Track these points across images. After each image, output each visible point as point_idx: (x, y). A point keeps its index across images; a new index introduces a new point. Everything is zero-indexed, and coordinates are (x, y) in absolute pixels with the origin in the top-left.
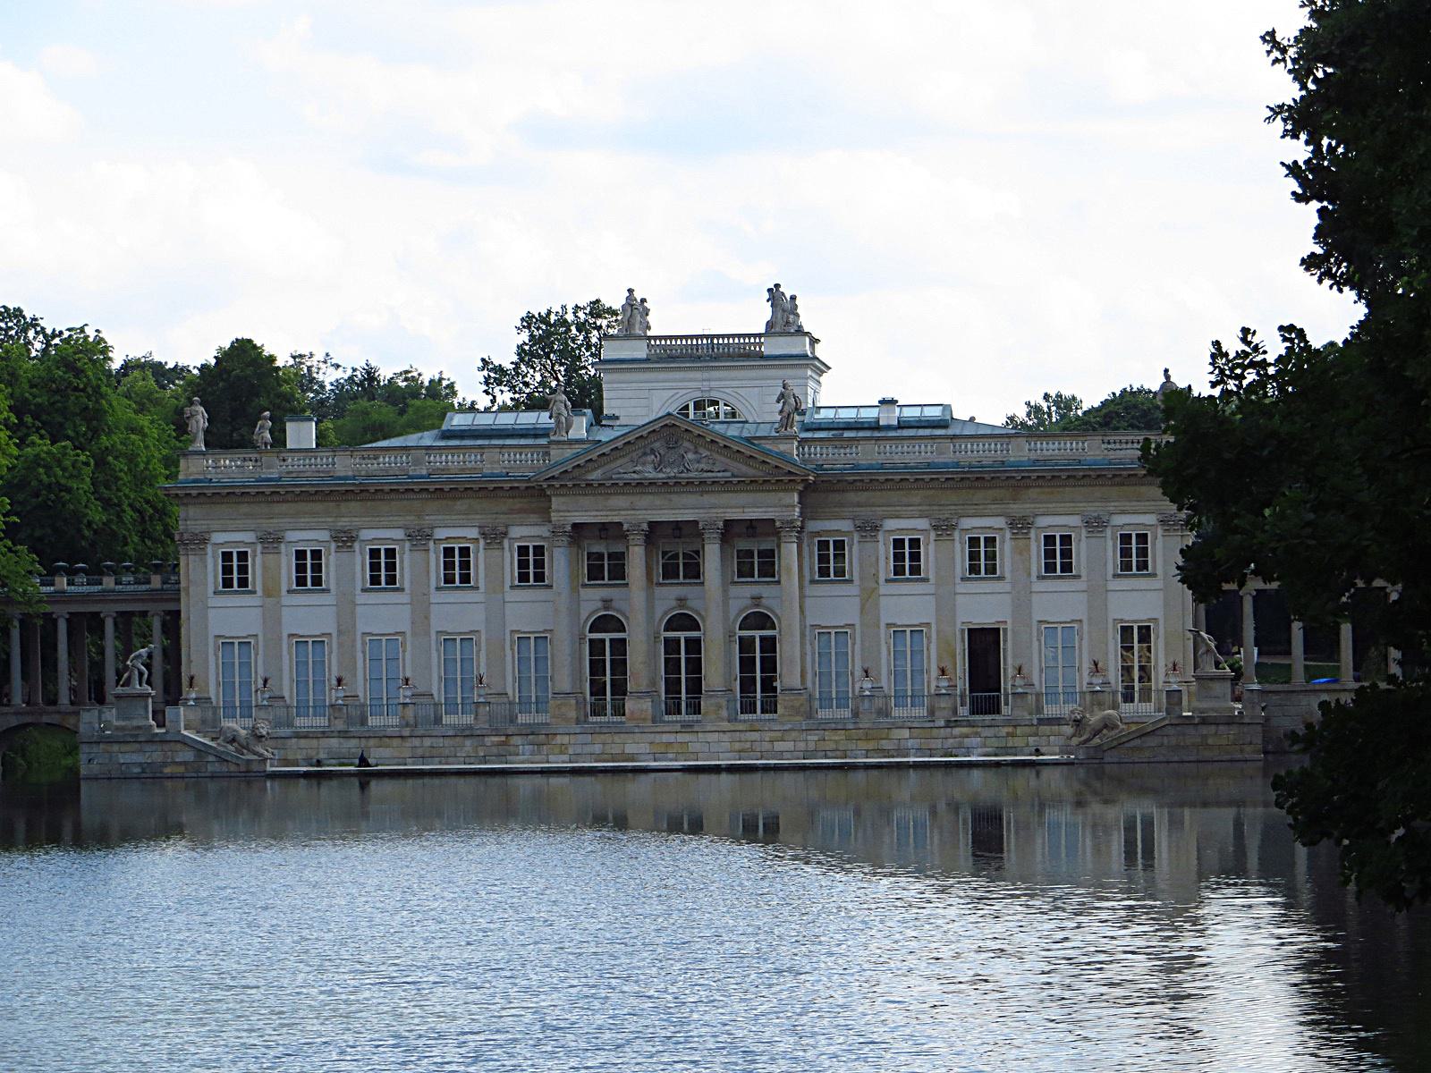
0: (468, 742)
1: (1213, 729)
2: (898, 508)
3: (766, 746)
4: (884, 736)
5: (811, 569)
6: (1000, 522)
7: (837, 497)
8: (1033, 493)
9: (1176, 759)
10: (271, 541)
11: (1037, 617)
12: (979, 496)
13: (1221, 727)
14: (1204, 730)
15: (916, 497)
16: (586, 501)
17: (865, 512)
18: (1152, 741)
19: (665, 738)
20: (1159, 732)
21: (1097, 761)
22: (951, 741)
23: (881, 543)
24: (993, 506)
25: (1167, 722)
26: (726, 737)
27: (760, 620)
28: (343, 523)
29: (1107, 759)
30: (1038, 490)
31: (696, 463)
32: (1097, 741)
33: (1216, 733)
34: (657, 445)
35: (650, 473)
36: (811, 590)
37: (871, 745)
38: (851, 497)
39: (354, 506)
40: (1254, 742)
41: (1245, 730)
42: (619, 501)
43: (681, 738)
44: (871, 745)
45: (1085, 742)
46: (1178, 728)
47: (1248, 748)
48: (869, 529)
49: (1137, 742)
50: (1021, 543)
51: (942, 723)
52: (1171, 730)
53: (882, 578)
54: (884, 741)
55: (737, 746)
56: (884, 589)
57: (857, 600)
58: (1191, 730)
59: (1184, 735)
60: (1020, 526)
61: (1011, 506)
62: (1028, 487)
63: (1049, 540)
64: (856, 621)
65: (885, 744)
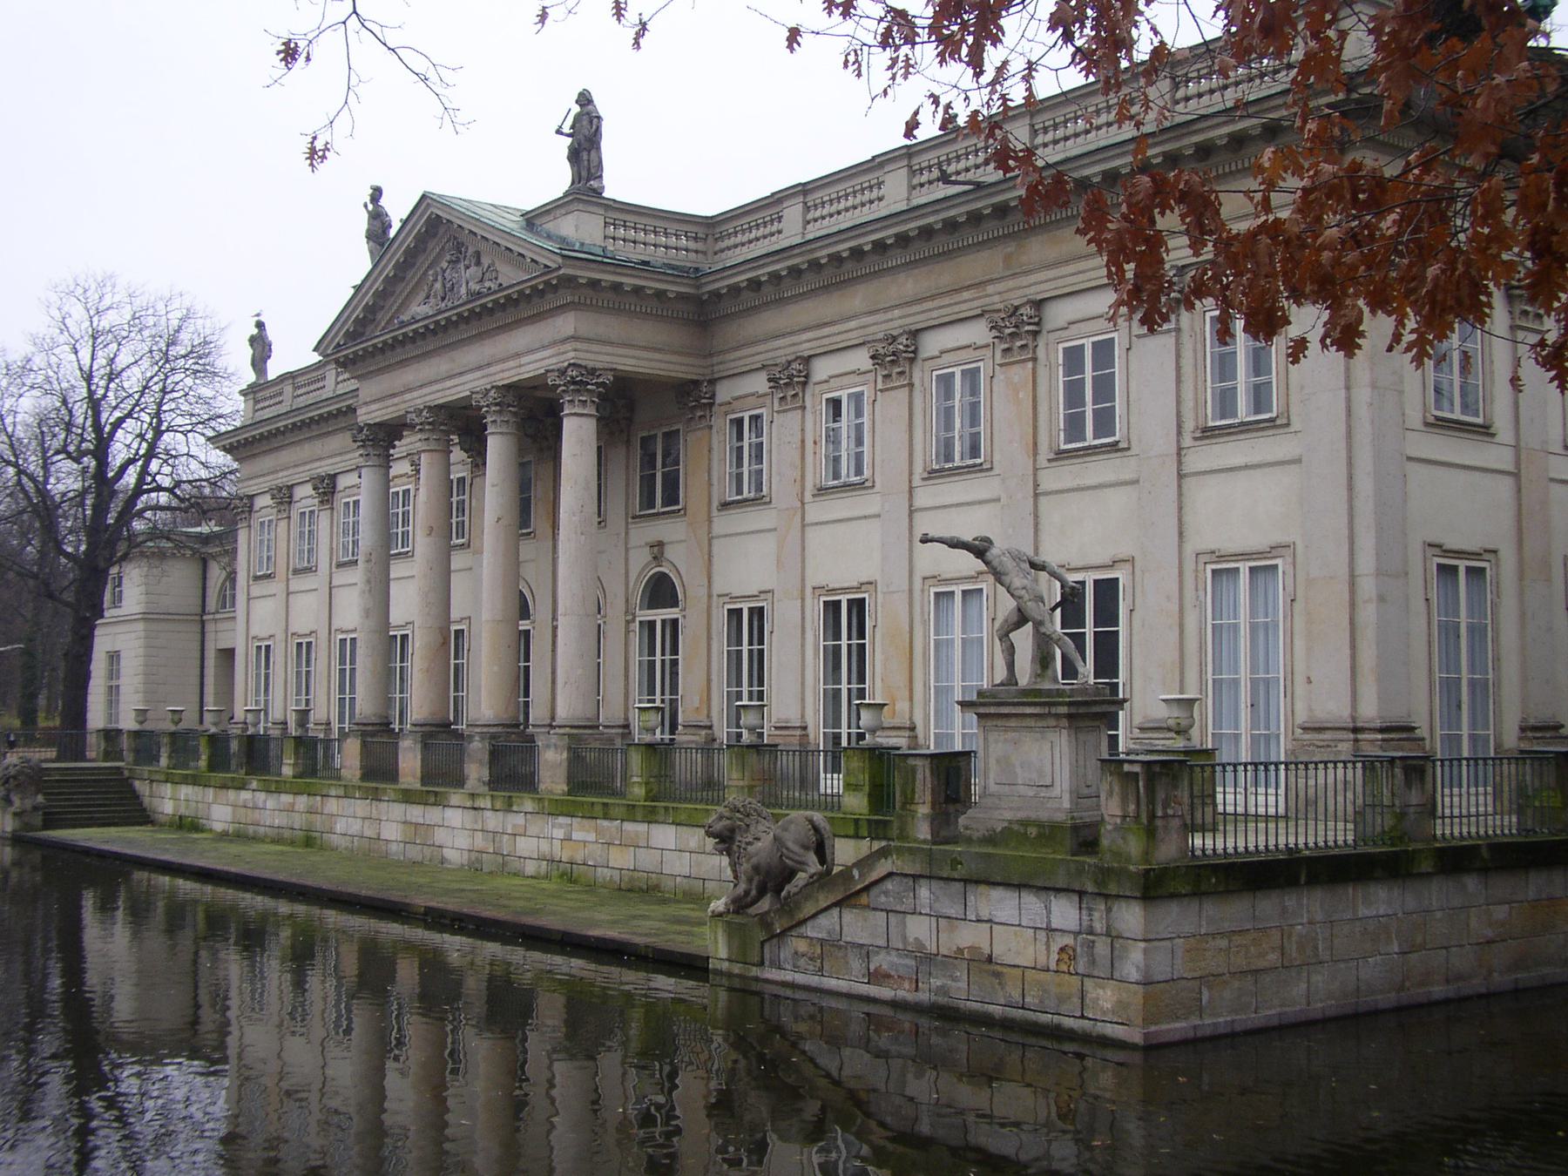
6: (978, 332)
8: (1038, 249)
10: (284, 497)
15: (856, 299)
17: (782, 350)
19: (416, 813)
27: (661, 591)
28: (325, 468)
32: (765, 904)
36: (725, 523)
42: (410, 375)
43: (433, 814)
48: (791, 381)
50: (1021, 373)
56: (815, 511)
63: (1073, 358)
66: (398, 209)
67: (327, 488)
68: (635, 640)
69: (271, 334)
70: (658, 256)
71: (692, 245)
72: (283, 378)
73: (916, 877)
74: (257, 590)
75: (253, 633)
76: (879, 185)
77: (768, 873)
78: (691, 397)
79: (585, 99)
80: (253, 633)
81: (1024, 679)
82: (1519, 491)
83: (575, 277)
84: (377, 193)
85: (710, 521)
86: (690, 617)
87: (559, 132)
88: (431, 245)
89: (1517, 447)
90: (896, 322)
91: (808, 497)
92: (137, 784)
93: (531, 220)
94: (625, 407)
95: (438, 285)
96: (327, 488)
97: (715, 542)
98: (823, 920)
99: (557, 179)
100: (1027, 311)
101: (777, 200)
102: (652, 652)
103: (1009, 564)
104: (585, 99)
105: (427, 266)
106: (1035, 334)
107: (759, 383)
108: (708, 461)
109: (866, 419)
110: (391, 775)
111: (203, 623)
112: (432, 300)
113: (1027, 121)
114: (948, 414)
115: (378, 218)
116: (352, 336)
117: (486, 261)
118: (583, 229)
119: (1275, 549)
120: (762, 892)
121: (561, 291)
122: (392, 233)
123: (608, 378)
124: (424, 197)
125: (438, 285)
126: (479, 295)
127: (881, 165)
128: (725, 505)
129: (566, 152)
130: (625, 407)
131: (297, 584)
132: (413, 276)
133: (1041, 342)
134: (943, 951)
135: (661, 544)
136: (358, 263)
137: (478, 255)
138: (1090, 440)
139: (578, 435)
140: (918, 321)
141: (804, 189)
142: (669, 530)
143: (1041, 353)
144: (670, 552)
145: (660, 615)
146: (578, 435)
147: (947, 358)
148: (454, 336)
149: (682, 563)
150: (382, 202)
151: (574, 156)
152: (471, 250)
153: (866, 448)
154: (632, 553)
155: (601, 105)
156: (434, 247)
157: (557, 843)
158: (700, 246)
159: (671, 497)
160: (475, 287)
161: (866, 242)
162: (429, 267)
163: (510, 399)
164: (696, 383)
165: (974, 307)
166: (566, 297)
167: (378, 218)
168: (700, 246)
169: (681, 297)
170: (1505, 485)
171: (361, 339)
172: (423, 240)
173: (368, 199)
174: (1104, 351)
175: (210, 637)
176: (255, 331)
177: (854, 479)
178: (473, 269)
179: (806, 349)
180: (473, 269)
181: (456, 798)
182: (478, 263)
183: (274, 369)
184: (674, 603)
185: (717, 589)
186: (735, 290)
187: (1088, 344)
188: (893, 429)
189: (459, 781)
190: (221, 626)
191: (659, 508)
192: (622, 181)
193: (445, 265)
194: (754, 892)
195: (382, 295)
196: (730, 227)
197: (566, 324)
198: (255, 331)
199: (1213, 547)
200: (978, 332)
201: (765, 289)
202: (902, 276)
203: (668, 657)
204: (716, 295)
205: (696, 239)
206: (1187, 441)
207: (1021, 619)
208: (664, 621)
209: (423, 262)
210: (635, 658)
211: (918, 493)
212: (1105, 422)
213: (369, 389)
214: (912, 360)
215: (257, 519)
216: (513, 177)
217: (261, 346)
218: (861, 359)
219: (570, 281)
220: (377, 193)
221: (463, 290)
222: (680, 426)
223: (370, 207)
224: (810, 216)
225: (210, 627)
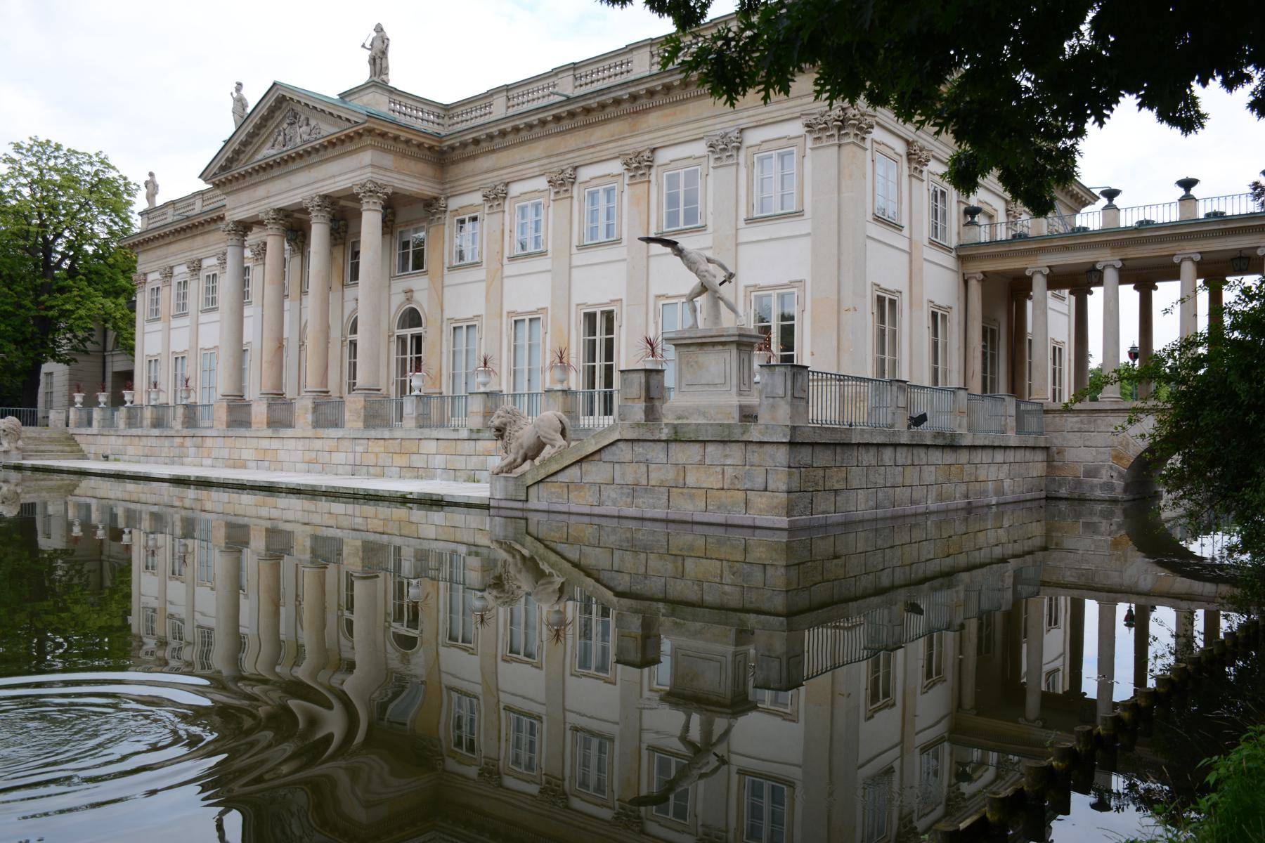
0: (167, 442)
1: (694, 451)
2: (520, 167)
3: (325, 457)
4: (415, 450)
5: (451, 253)
7: (469, 166)
8: (653, 119)
9: (632, 512)
10: (168, 274)
11: (655, 291)
12: (599, 134)
13: (711, 448)
14: (683, 454)
15: (538, 149)
16: (244, 196)
17: (493, 179)
18: (596, 472)
19: (265, 443)
20: (606, 455)
21: (519, 505)
22: (474, 459)
23: (507, 215)
24: (610, 145)
25: (616, 436)
26: (300, 444)
27: (412, 318)
28: (196, 255)
29: (534, 503)
30: (658, 113)
31: (301, 135)
32: (527, 466)
33: (701, 463)
34: (285, 125)
35: (268, 152)
36: (451, 278)
37: (401, 461)
38: (484, 163)
39: (199, 241)
40: (771, 486)
41: (755, 458)
42: (261, 191)
43: (275, 444)
44: (403, 461)
45: (511, 467)
46: (639, 449)
47: (759, 501)
48: (497, 197)
49: (574, 473)
51: (464, 434)
52: (624, 452)
53: (506, 254)
54: (414, 457)
55: (308, 456)
56: (510, 269)
57: (484, 284)
58: (657, 453)
59: (647, 463)
60: (640, 165)
61: (629, 141)
62: (646, 111)
63: (673, 181)
64: (481, 311)
65: (417, 461)
66: (253, 97)
67: (196, 267)
68: (394, 346)
69: (158, 180)
70: (419, 125)
71: (436, 120)
72: (166, 205)
73: (632, 441)
74: (149, 328)
75: (146, 353)
76: (554, 86)
77: (529, 448)
78: (430, 207)
79: (379, 29)
80: (146, 353)
81: (701, 325)
82: (911, 261)
83: (374, 129)
84: (240, 85)
85: (443, 276)
86: (428, 332)
87: (363, 46)
88: (277, 114)
89: (910, 239)
90: (565, 163)
91: (505, 261)
92: (77, 438)
93: (343, 96)
94: (395, 210)
95: (281, 138)
96: (196, 267)
97: (446, 290)
98: (568, 472)
99: (362, 74)
100: (647, 154)
101: (490, 94)
102: (404, 352)
103: (694, 256)
104: (379, 29)
105: (274, 126)
106: (650, 167)
107: (477, 198)
108: (444, 241)
109: (542, 217)
110: (246, 424)
111: (104, 357)
112: (277, 147)
113: (648, 49)
114: (594, 213)
115: (240, 102)
116: (223, 169)
117: (313, 123)
118: (380, 104)
119: (792, 284)
120: (524, 460)
121: (364, 138)
122: (249, 110)
123: (389, 190)
124: (274, 84)
125: (281, 138)
126: (309, 141)
127: (556, 74)
128: (451, 268)
129: (367, 59)
130: (395, 210)
131: (175, 323)
132: (264, 132)
133: (653, 171)
134: (653, 483)
135: (411, 291)
136: (227, 127)
137: (308, 119)
138: (682, 226)
139: (371, 221)
140: (579, 161)
141: (507, 88)
142: (419, 284)
143: (653, 178)
144: (417, 296)
145: (409, 332)
146: (371, 221)
147: (594, 182)
148: (291, 166)
149: (423, 303)
150: (243, 92)
151: (373, 61)
152: (303, 117)
153: (542, 234)
154: (393, 298)
155: (389, 33)
156: (279, 116)
157: (358, 456)
158: (440, 121)
159: (419, 264)
160: (305, 137)
161: (548, 115)
162: (277, 127)
163: (326, 203)
164: (437, 199)
165: (615, 152)
166: (368, 140)
167: (240, 102)
168: (440, 121)
169: (431, 148)
170: (905, 257)
171: (229, 170)
172: (272, 111)
173: (234, 90)
174: (691, 178)
175: (109, 365)
176: (148, 178)
177: (533, 250)
178: (304, 128)
179: (506, 178)
180: (304, 128)
181: (288, 432)
182: (308, 124)
183: (159, 201)
184: (419, 324)
185: (447, 315)
186: (464, 145)
187: (682, 172)
188: (558, 221)
189: (290, 425)
190: (116, 358)
191: (410, 271)
192: (396, 79)
193: (285, 125)
194: (519, 460)
195: (245, 144)
196: (459, 110)
197: (367, 157)
198: (148, 178)
199: (753, 283)
200: (616, 167)
201: (484, 144)
202: (568, 137)
203: (414, 355)
204: (452, 148)
205: (438, 117)
206: (742, 224)
207: (704, 289)
208: (412, 336)
209: (272, 124)
210: (394, 357)
211: (574, 257)
212: (691, 215)
213: (229, 201)
214: (573, 183)
215: (148, 288)
216: (331, 73)
217: (152, 187)
218: (542, 183)
219: (370, 131)
220: (240, 85)
221: (298, 140)
222: (425, 224)
223: (235, 95)
224: (511, 103)
225: (109, 359)
